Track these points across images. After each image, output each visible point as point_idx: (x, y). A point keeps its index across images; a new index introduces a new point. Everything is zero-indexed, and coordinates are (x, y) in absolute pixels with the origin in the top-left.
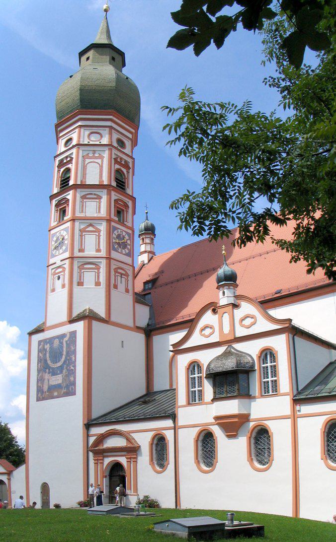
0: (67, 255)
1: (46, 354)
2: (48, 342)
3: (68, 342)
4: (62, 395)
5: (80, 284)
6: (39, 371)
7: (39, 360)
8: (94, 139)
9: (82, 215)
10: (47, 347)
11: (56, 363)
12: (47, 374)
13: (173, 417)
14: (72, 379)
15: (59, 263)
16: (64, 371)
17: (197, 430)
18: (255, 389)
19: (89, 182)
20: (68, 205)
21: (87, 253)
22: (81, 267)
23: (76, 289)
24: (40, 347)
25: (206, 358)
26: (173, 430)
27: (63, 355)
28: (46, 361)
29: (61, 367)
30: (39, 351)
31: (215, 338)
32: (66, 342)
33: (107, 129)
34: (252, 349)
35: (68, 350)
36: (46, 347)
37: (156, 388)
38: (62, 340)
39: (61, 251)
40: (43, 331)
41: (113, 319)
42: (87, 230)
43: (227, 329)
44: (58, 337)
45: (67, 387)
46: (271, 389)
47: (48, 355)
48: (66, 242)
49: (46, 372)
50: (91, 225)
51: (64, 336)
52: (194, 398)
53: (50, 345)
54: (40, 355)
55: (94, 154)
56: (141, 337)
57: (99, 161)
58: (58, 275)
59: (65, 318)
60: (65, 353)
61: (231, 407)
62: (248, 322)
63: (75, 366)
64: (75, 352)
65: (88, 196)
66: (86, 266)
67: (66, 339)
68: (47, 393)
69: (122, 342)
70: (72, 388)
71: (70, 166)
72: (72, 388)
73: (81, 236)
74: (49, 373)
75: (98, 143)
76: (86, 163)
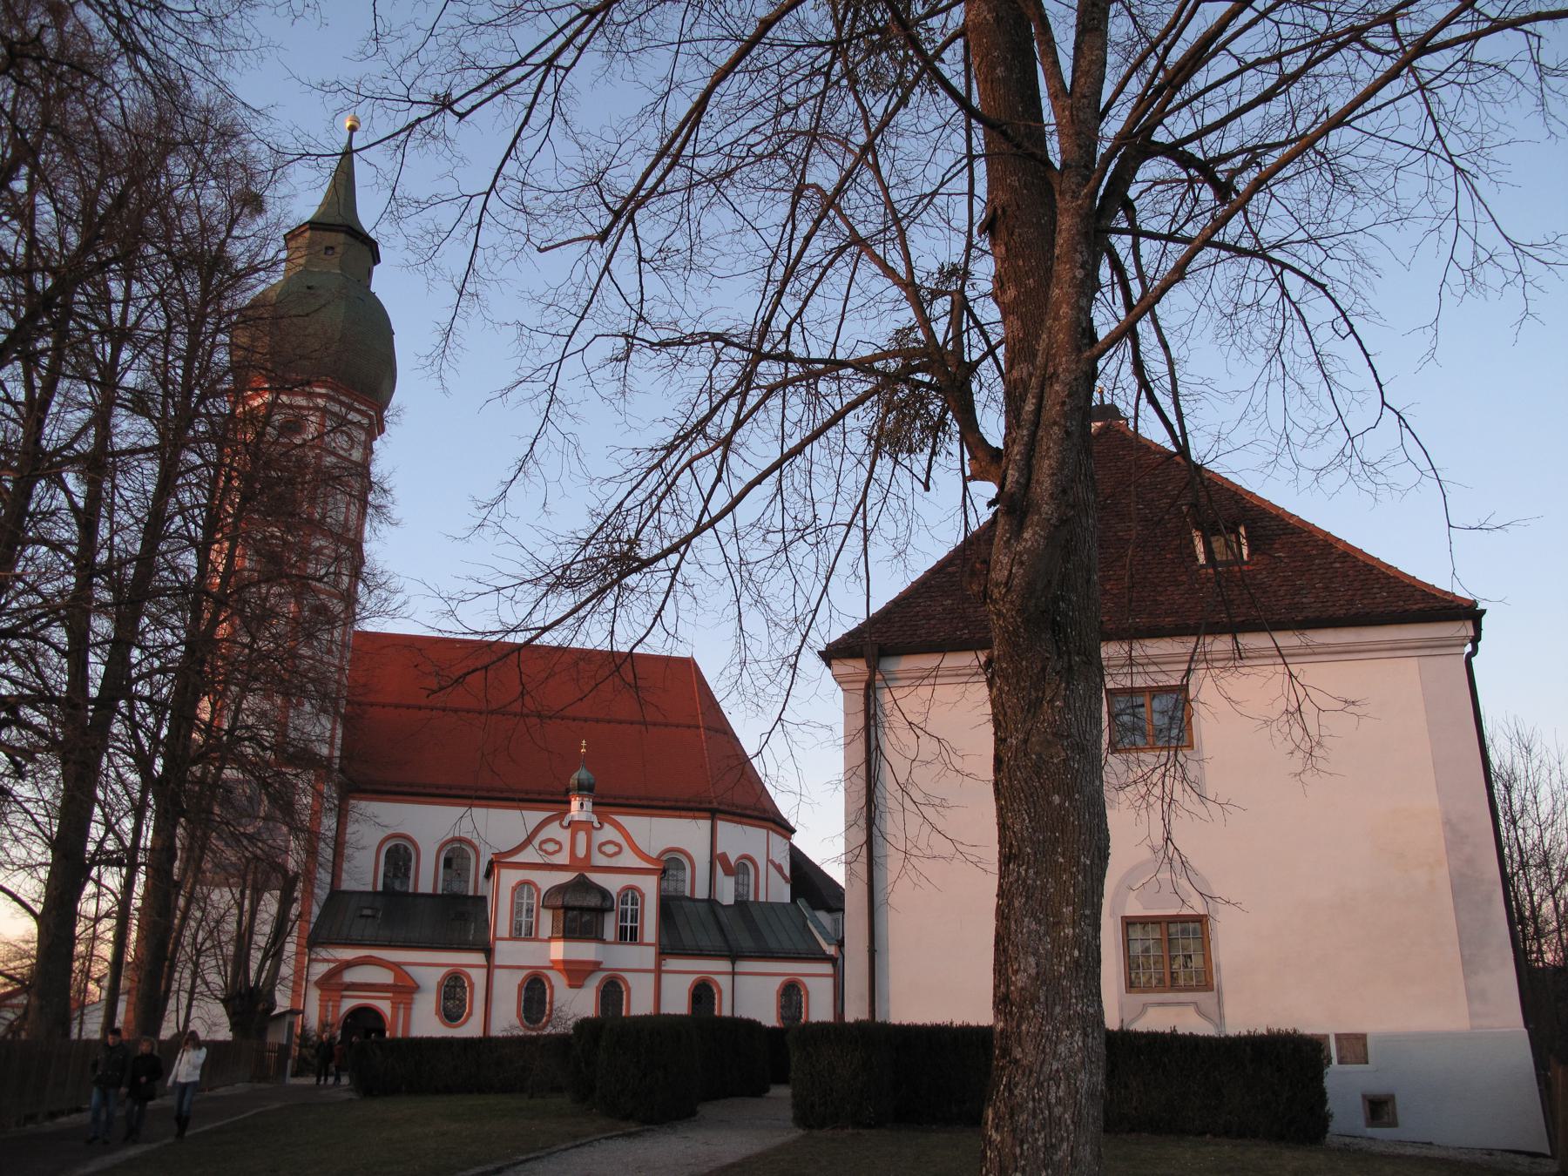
13: (489, 952)
17: (526, 972)
18: (610, 931)
25: (547, 881)
26: (485, 970)
31: (563, 858)
34: (613, 884)
43: (581, 852)
46: (629, 935)
52: (523, 932)
61: (585, 951)
62: (610, 849)
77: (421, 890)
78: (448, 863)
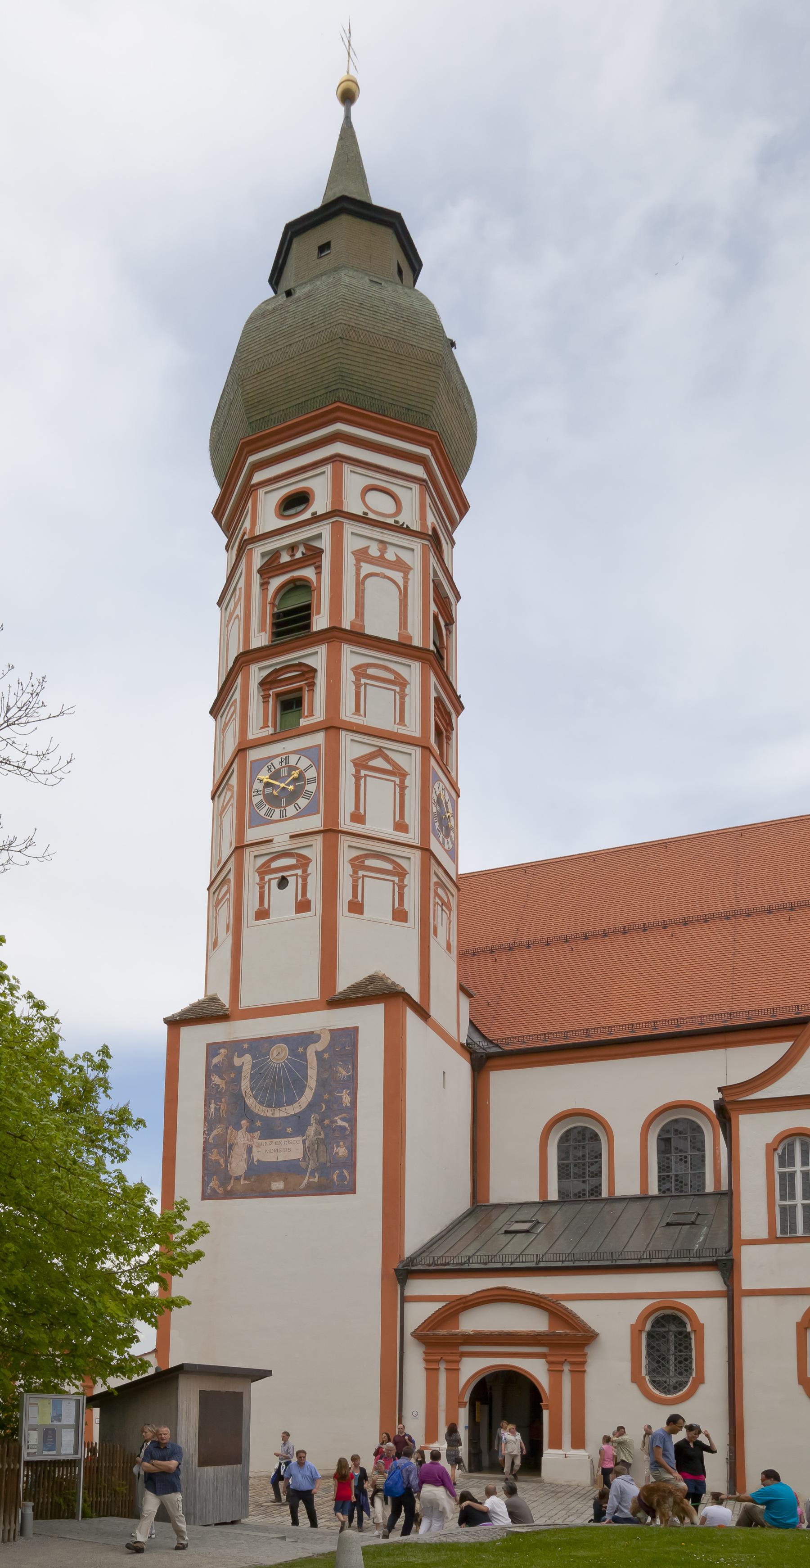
0: (316, 822)
1: (238, 1080)
2: (248, 1051)
3: (326, 1056)
4: (304, 1189)
5: (356, 907)
6: (210, 1122)
7: (211, 1094)
8: (381, 504)
9: (358, 720)
10: (246, 1062)
11: (279, 1105)
12: (240, 1133)
14: (342, 1151)
15: (281, 842)
16: (311, 1130)
19: (371, 629)
20: (312, 685)
21: (370, 827)
22: (357, 864)
23: (346, 921)
24: (215, 1060)
27: (305, 1086)
28: (238, 1098)
29: (299, 1124)
30: (210, 1071)
32: (318, 1054)
33: (416, 487)
35: (326, 1075)
36: (237, 1061)
37: (495, 1197)
38: (301, 1050)
39: (291, 810)
40: (224, 1017)
41: (433, 1012)
42: (372, 763)
44: (285, 1039)
45: (323, 1169)
47: (245, 1084)
48: (311, 788)
49: (238, 1127)
50: (380, 753)
51: (310, 1037)
53: (254, 1057)
54: (216, 1080)
55: (383, 551)
56: (463, 1068)
57: (398, 576)
58: (280, 875)
59: (312, 991)
60: (312, 1082)
63: (353, 1121)
64: (352, 1084)
65: (370, 671)
66: (369, 862)
67: (320, 1046)
68: (243, 1182)
69: (444, 1073)
70: (341, 1177)
71: (308, 573)
72: (341, 1177)
73: (357, 778)
74: (251, 1130)
75: (391, 521)
76: (363, 574)
77: (619, 1192)
78: (665, 1143)
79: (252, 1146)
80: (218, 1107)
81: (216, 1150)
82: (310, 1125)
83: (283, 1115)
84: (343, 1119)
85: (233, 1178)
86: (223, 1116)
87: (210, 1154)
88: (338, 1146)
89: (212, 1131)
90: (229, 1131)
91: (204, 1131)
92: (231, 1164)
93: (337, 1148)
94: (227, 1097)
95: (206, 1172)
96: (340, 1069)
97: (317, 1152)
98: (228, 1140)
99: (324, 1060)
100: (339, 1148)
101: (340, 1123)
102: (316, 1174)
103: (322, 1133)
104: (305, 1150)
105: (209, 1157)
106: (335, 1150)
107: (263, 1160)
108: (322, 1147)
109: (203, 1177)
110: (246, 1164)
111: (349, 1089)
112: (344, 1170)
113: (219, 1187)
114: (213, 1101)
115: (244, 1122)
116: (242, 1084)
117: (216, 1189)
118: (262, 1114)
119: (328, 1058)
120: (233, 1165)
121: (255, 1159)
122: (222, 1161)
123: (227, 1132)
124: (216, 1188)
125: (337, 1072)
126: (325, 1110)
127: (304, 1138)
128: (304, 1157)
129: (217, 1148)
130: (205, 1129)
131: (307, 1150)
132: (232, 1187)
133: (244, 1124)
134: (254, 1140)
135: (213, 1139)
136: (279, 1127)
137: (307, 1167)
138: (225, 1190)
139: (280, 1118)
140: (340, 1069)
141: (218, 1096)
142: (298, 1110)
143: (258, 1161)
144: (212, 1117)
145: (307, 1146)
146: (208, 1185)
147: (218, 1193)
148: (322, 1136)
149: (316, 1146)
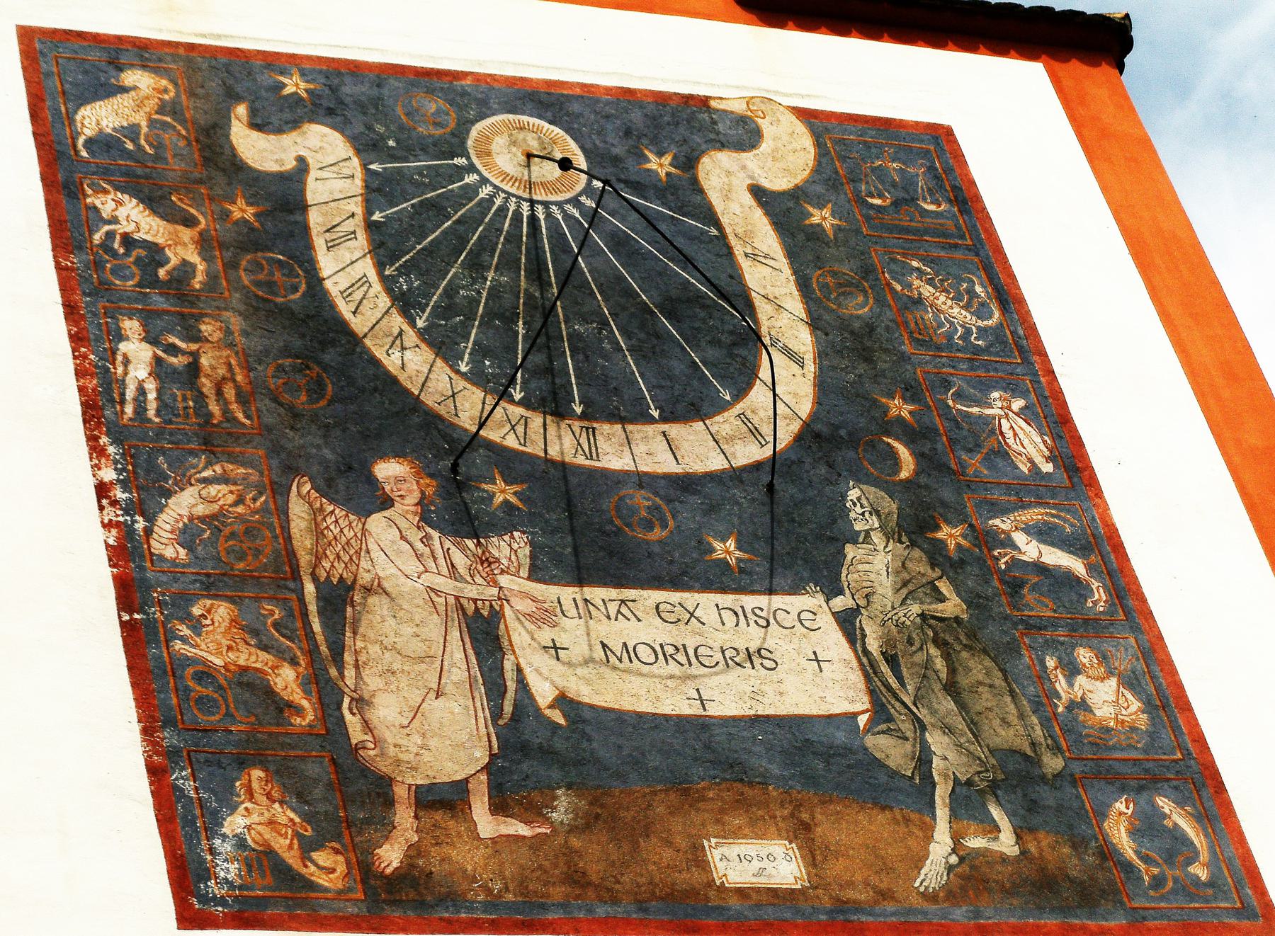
68: (486, 824)
79: (496, 616)
80: (176, 361)
81: (223, 611)
82: (855, 542)
83: (665, 464)
84: (1043, 533)
85: (400, 792)
86: (228, 416)
87: (185, 631)
88: (1072, 669)
89: (168, 494)
90: (298, 511)
91: (102, 490)
92: (361, 703)
93: (1071, 685)
94: (236, 323)
95: (168, 737)
96: (927, 291)
97: (951, 688)
98: (304, 559)
99: (815, 234)
100: (1080, 680)
101: (1030, 549)
102: (996, 812)
103: (944, 587)
104: (869, 670)
105: (178, 645)
106: (1061, 685)
107: (599, 701)
108: (977, 669)
109: (155, 772)
110: (484, 714)
111: (1024, 394)
112: (1164, 804)
113: (307, 847)
114: (131, 326)
115: (388, 470)
116: (327, 263)
117: (292, 858)
118: (511, 442)
119: (838, 229)
120: (387, 711)
121: (543, 693)
122: (286, 680)
123: (283, 512)
124: (281, 844)
125: (919, 301)
126: (917, 473)
127: (839, 603)
128: (880, 712)
129: (231, 600)
130: (109, 475)
131: (885, 668)
132: (414, 851)
133: (399, 480)
134: (504, 580)
135: (187, 535)
136: (649, 526)
137: (923, 760)
138: (364, 869)
139: (644, 480)
140: (927, 291)
141: (159, 301)
142: (749, 453)
143: (562, 701)
144: (140, 409)
145: (873, 645)
146: (213, 826)
147: (310, 885)
148: (952, 605)
149: (934, 651)
